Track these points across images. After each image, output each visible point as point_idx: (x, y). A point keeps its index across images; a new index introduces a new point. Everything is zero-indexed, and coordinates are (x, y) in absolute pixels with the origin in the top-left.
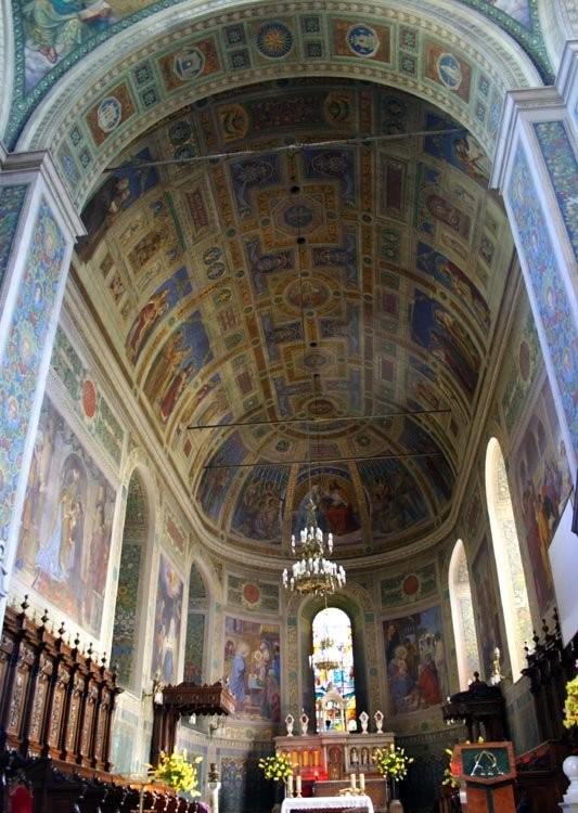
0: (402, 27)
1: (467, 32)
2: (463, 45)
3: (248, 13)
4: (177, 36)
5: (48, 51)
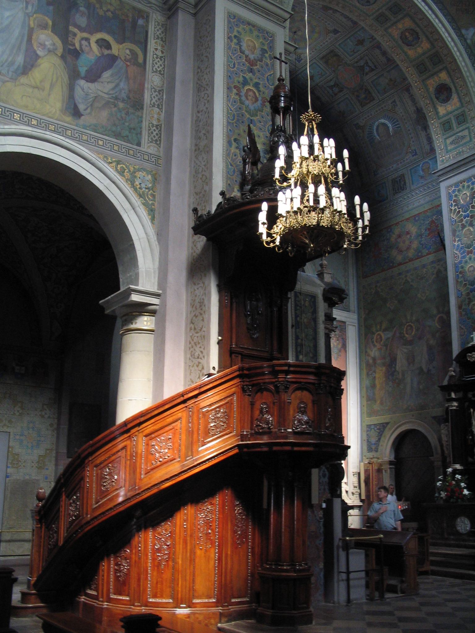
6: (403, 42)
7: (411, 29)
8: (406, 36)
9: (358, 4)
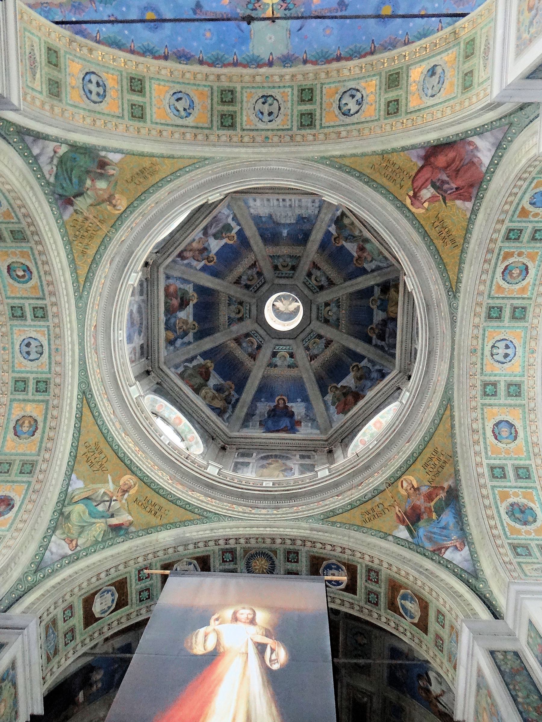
0: (367, 566)
1: (420, 573)
2: (419, 583)
3: (242, 541)
4: (181, 549)
5: (72, 541)
6: (15, 428)
7: (36, 421)
8: (24, 423)
9: (17, 347)
